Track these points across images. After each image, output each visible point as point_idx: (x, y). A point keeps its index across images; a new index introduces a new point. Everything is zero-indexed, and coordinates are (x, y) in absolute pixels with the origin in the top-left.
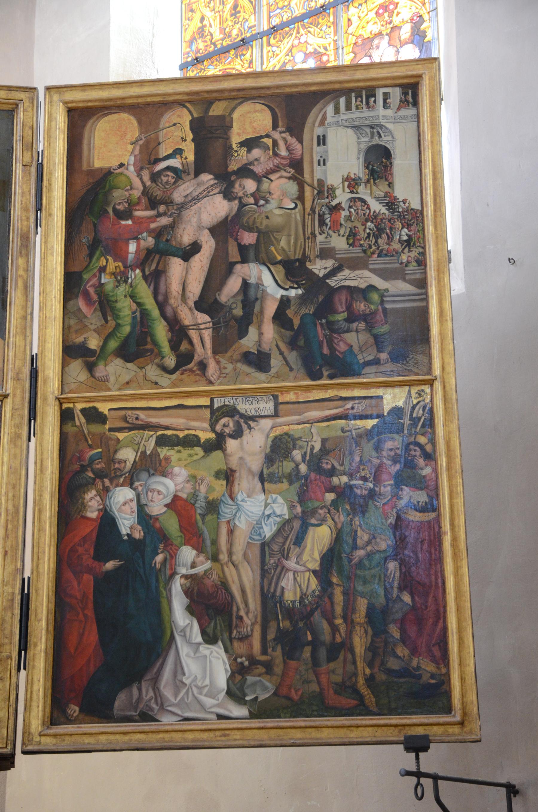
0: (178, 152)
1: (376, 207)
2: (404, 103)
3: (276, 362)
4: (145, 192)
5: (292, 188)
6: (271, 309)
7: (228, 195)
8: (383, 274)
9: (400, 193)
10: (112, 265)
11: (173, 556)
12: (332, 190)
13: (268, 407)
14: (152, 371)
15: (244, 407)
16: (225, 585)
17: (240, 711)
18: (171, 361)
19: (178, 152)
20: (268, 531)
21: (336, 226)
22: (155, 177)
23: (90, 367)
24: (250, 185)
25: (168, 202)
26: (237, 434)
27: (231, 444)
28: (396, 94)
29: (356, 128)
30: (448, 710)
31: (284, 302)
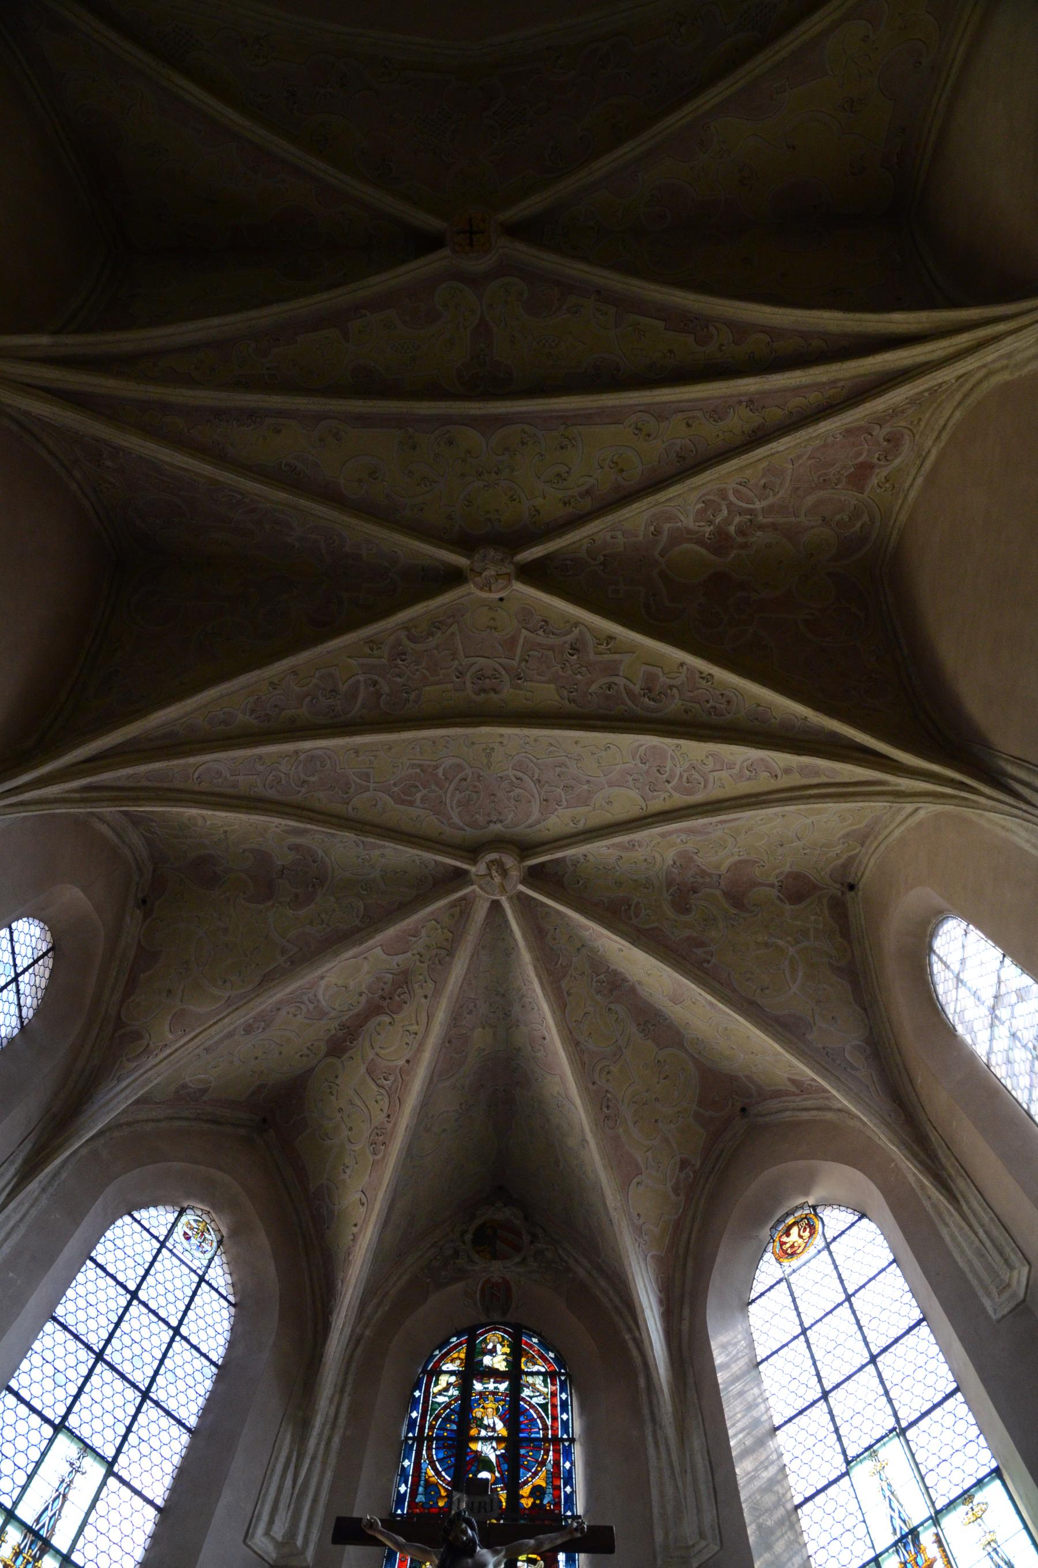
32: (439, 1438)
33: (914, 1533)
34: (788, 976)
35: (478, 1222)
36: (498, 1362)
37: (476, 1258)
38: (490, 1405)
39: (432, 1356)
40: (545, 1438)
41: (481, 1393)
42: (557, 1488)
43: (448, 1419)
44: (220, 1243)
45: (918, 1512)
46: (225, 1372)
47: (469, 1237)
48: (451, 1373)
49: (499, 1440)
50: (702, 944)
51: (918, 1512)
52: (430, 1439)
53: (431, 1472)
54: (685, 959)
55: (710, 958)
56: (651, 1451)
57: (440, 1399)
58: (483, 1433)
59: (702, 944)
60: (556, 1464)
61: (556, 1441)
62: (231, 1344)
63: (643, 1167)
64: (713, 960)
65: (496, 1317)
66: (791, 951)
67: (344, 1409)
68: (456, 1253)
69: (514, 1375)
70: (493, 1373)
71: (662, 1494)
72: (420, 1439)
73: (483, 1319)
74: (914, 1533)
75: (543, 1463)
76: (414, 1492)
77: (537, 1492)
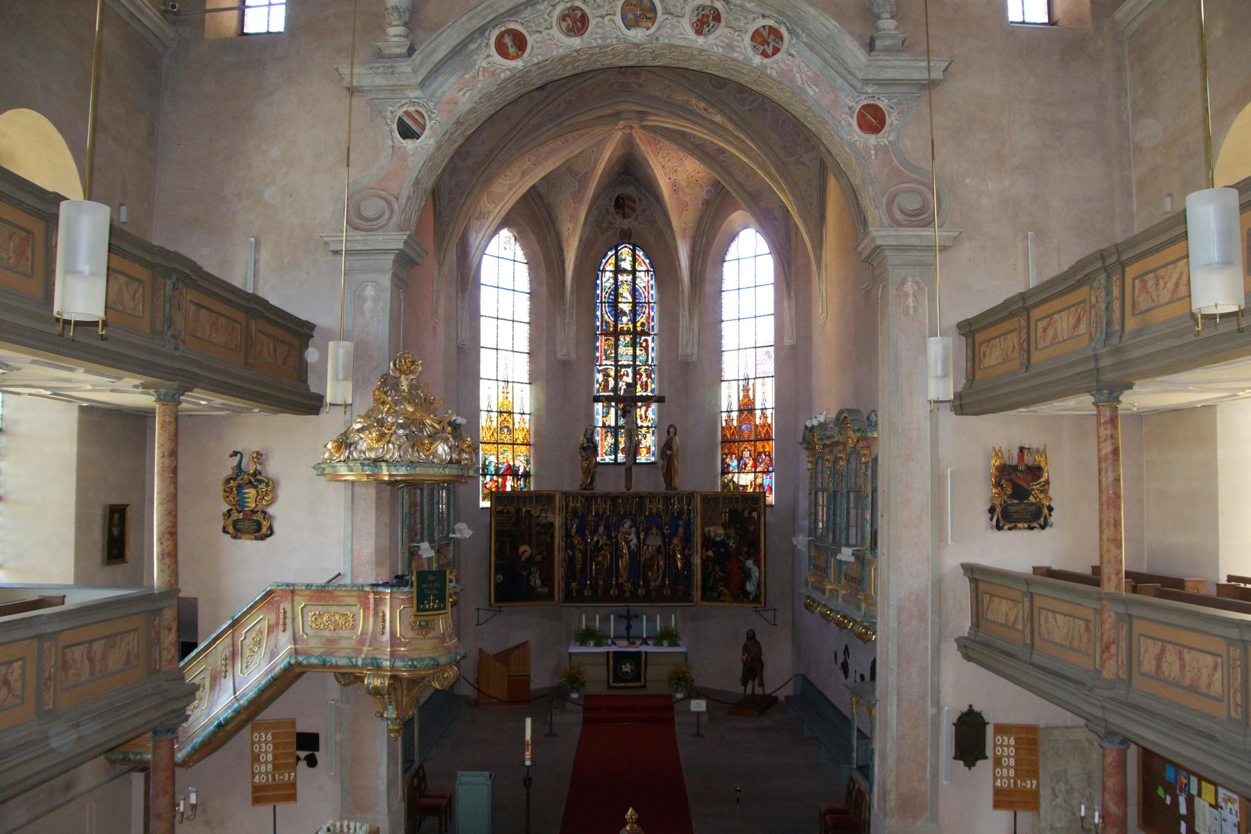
32: (608, 302)
33: (748, 379)
35: (616, 196)
36: (626, 265)
37: (618, 218)
38: (625, 287)
39: (602, 262)
40: (645, 303)
41: (622, 281)
42: (649, 323)
43: (610, 294)
44: (516, 240)
45: (752, 375)
46: (533, 295)
47: (613, 204)
48: (611, 271)
49: (629, 303)
51: (752, 375)
52: (605, 302)
53: (606, 317)
56: (681, 319)
57: (608, 285)
58: (624, 300)
60: (649, 314)
61: (649, 303)
62: (531, 282)
63: (688, 201)
65: (626, 241)
67: (575, 299)
68: (608, 211)
69: (634, 272)
70: (625, 271)
71: (683, 336)
72: (601, 303)
73: (621, 242)
74: (748, 379)
75: (644, 313)
76: (602, 326)
77: (643, 325)
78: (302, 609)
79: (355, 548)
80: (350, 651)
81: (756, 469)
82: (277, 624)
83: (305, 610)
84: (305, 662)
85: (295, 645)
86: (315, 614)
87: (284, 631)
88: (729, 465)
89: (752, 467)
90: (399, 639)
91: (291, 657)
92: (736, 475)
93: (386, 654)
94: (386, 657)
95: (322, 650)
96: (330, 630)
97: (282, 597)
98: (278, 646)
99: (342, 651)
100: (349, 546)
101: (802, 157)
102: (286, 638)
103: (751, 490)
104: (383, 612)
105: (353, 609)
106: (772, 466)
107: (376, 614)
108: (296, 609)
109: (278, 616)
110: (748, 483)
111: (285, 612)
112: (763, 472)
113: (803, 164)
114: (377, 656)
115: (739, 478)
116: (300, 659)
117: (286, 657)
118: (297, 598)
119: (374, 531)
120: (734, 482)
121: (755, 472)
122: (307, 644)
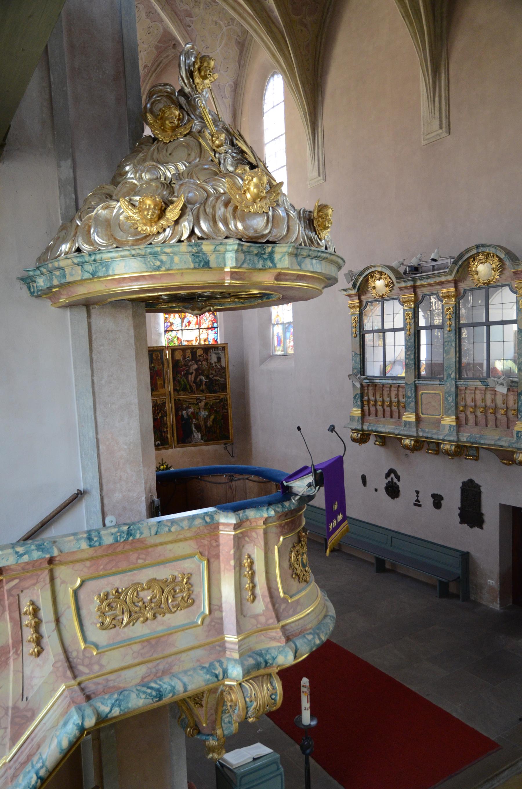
0: (189, 357)
1: (219, 367)
2: (223, 350)
3: (205, 391)
4: (184, 364)
5: (206, 363)
6: (204, 383)
7: (197, 365)
8: (221, 378)
9: (222, 365)
10: (180, 376)
11: (192, 420)
12: (212, 364)
13: (204, 398)
14: (187, 393)
15: (201, 398)
16: (200, 424)
17: (202, 441)
18: (190, 391)
19: (189, 357)
20: (205, 416)
21: (213, 370)
22: (186, 361)
23: (178, 392)
24: (200, 363)
25: (188, 365)
26: (200, 402)
27: (200, 404)
28: (221, 348)
29: (216, 354)
30: (229, 439)
31: (206, 382)
34: (218, 43)
50: (190, 16)
54: (181, 22)
55: (191, 24)
59: (190, 16)
64: (192, 27)
66: (225, 29)
78: (76, 593)
79: (100, 436)
80: (199, 653)
81: (200, 326)
82: (19, 642)
83: (82, 595)
84: (116, 712)
85: (75, 677)
86: (107, 595)
87: (39, 654)
88: (172, 324)
89: (197, 324)
90: (284, 600)
91: (79, 709)
92: (180, 331)
93: (274, 639)
94: (274, 644)
95: (142, 670)
96: (147, 619)
97: (22, 579)
98: (30, 693)
99: (183, 656)
100: (92, 434)
101: (305, 19)
102: (49, 668)
103: (197, 344)
104: (249, 557)
105: (188, 565)
106: (216, 322)
107: (239, 565)
108: (60, 597)
109: (19, 625)
110: (194, 339)
111: (36, 612)
112: (208, 328)
113: (305, 26)
114: (259, 647)
115: (182, 334)
116: (105, 709)
117: (66, 712)
118: (61, 572)
119: (136, 401)
120: (178, 338)
121: (199, 329)
122: (102, 666)
